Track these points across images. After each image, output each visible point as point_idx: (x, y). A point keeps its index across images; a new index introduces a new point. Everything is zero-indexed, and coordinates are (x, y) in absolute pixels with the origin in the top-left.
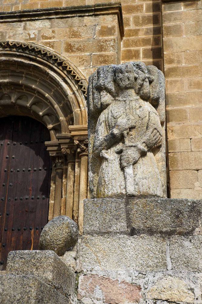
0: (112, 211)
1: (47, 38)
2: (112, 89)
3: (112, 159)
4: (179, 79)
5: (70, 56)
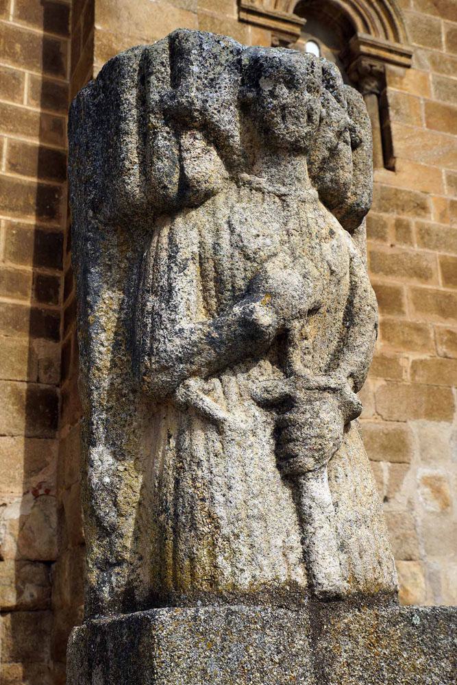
0: (268, 665)
2: (232, 137)
3: (243, 426)
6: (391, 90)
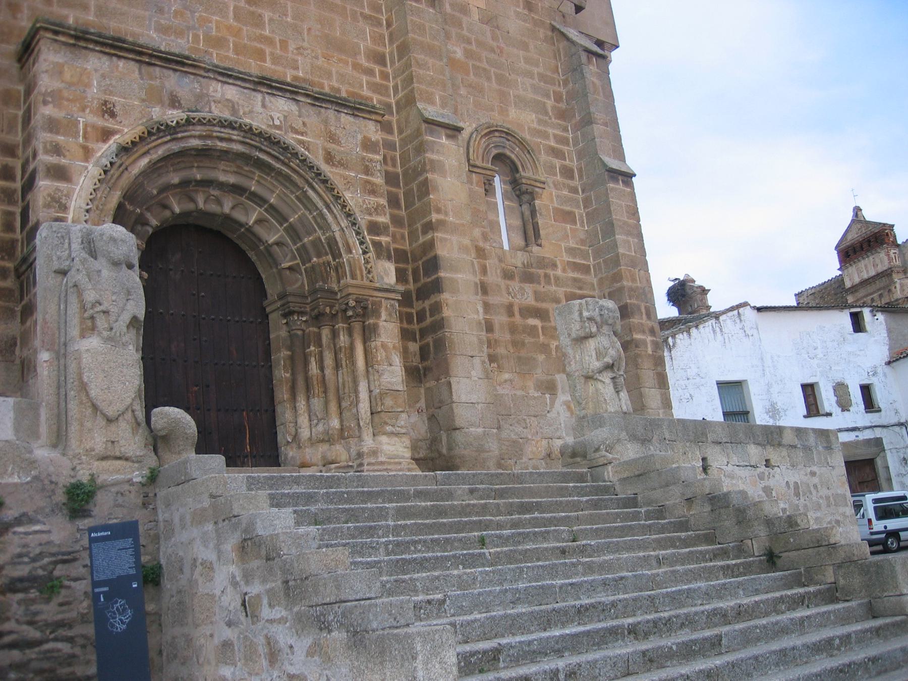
4: (448, 237)
5: (331, 172)
6: (537, 202)
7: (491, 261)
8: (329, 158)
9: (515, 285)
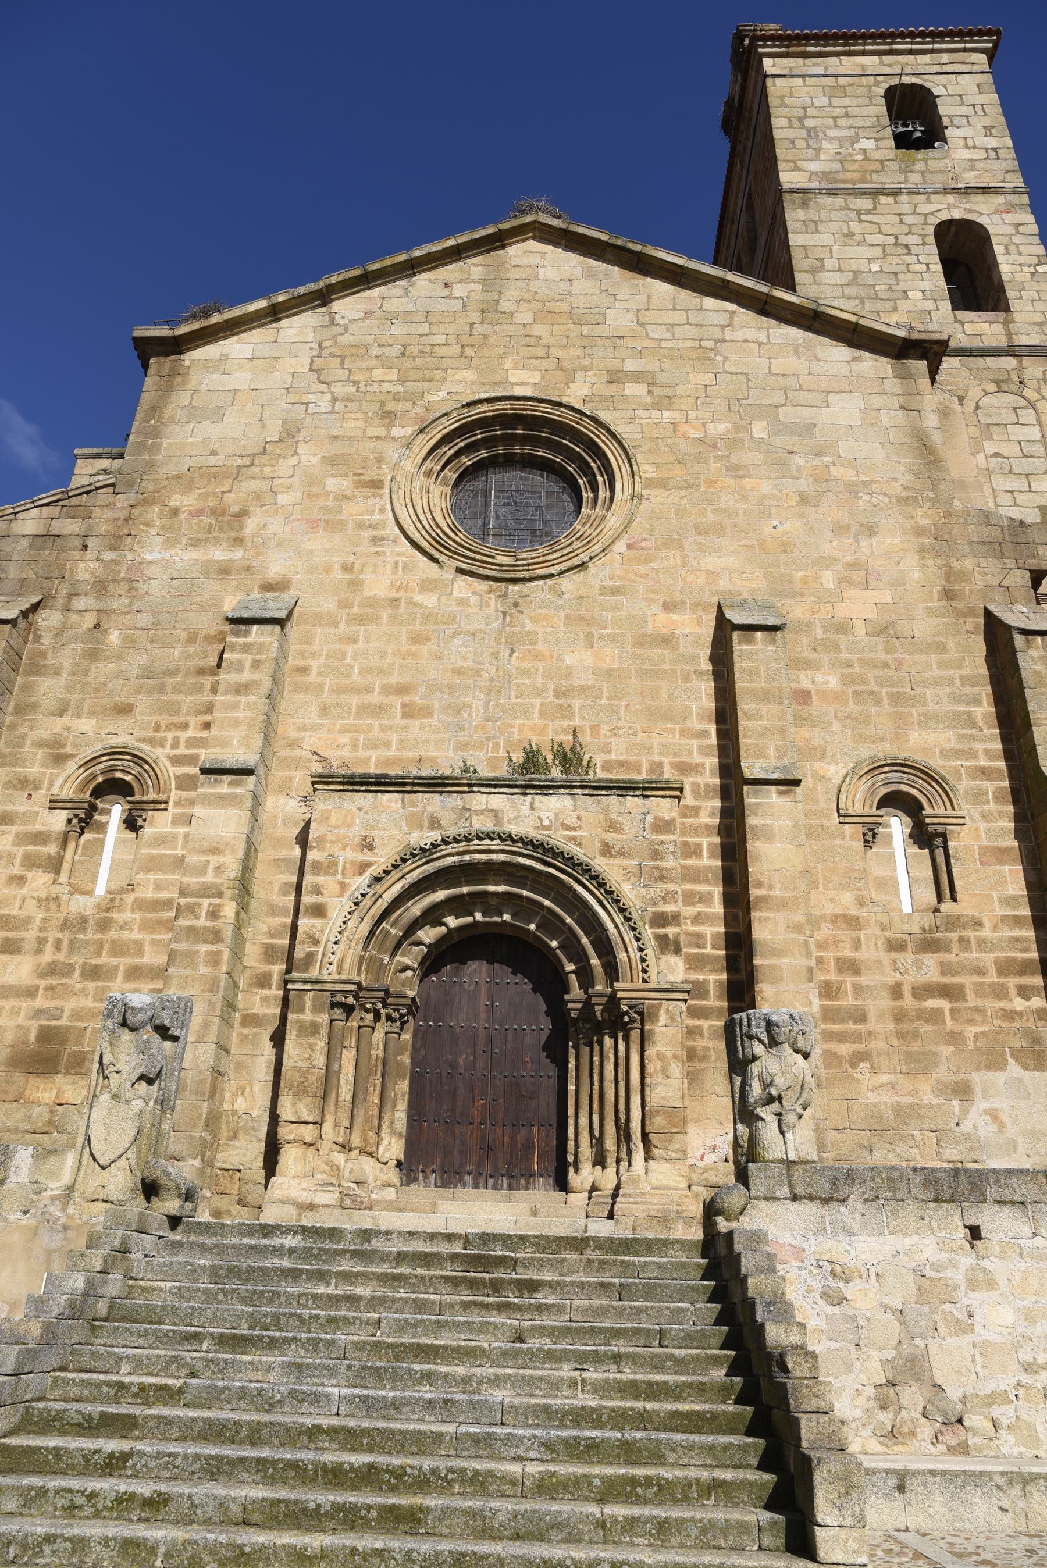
1: (568, 828)
4: (771, 915)
6: (951, 844)
7: (869, 931)
8: (606, 850)
9: (907, 958)
